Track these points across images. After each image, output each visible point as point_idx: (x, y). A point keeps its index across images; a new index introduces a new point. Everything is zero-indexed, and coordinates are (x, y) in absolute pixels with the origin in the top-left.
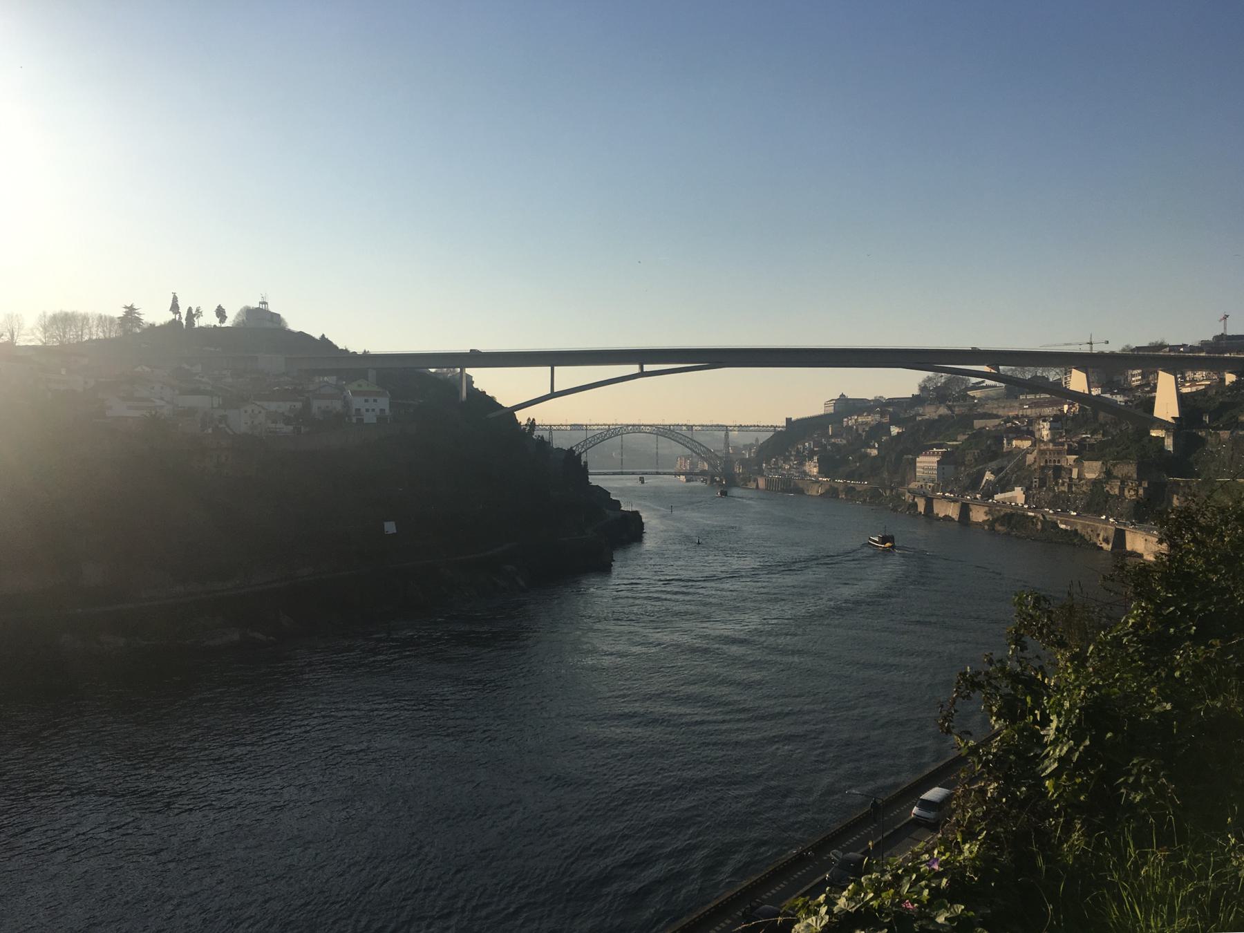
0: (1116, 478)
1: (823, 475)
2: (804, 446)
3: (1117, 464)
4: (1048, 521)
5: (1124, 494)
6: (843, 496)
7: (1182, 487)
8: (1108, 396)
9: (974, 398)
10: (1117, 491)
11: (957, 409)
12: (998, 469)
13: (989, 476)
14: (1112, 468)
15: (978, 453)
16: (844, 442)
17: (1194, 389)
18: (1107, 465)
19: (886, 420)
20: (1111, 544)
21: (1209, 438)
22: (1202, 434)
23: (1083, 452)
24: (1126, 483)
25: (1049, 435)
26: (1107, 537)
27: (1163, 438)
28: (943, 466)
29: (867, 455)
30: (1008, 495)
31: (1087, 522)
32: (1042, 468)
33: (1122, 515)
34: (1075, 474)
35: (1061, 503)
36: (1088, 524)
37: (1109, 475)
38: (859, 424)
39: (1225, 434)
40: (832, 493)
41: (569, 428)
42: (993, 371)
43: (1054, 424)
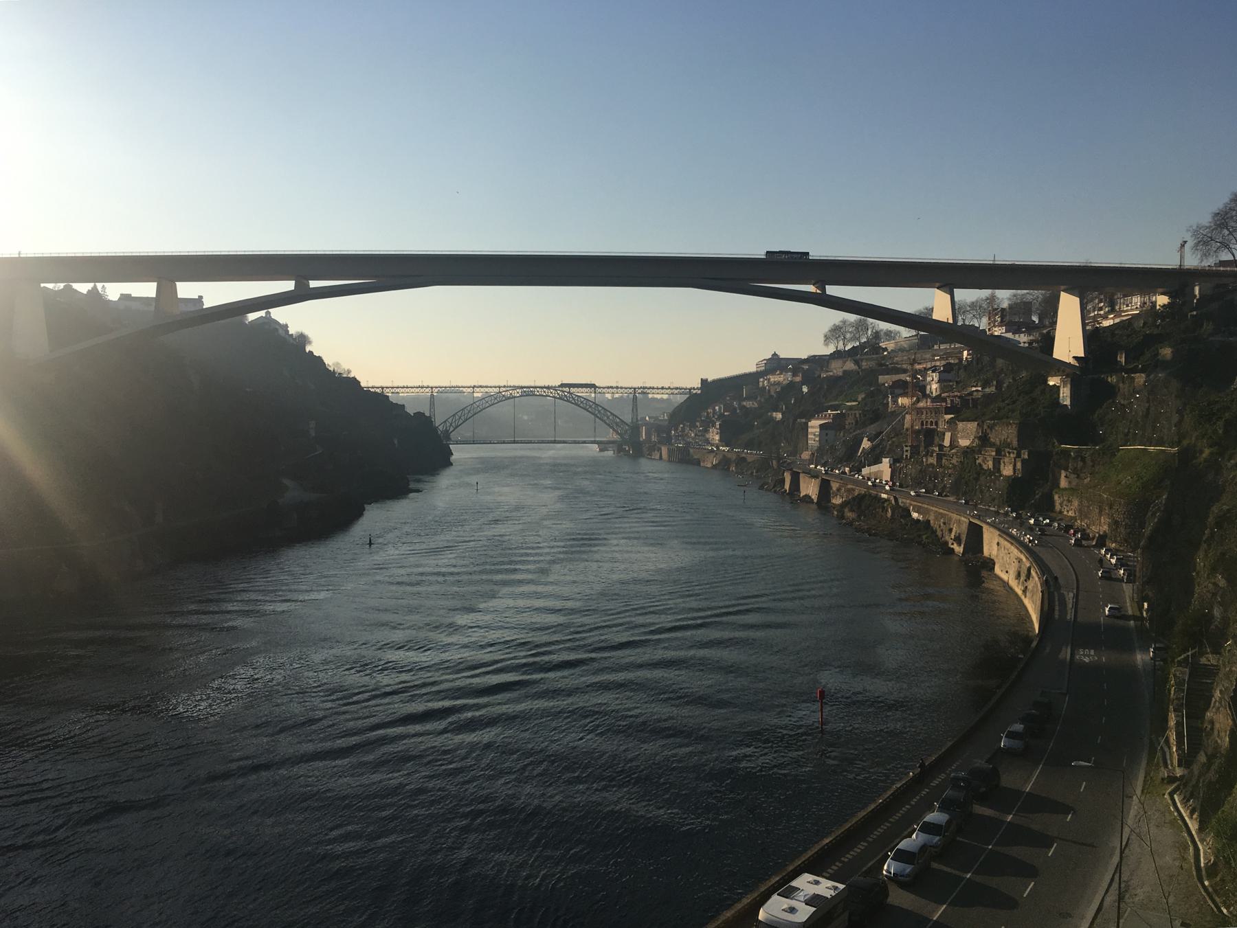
0: (992, 445)
1: (724, 443)
2: (714, 410)
3: (994, 425)
4: (901, 507)
5: (999, 469)
6: (734, 469)
7: (1074, 458)
8: (1010, 335)
9: (885, 349)
10: (990, 464)
11: (864, 364)
12: (875, 435)
13: (866, 444)
14: (988, 431)
15: (860, 414)
16: (756, 405)
17: (1117, 320)
18: (983, 428)
19: (798, 379)
20: (962, 546)
21: (1121, 385)
22: (1112, 379)
23: (962, 410)
24: (1003, 453)
25: (938, 390)
26: (959, 534)
27: (1059, 387)
28: (827, 432)
29: (773, 419)
30: (874, 468)
31: (941, 511)
32: (918, 432)
33: (994, 500)
34: (947, 443)
35: (925, 480)
36: (942, 513)
37: (984, 440)
38: (771, 385)
39: (1140, 379)
40: (724, 465)
41: (517, 393)
42: (818, 291)
43: (946, 374)
